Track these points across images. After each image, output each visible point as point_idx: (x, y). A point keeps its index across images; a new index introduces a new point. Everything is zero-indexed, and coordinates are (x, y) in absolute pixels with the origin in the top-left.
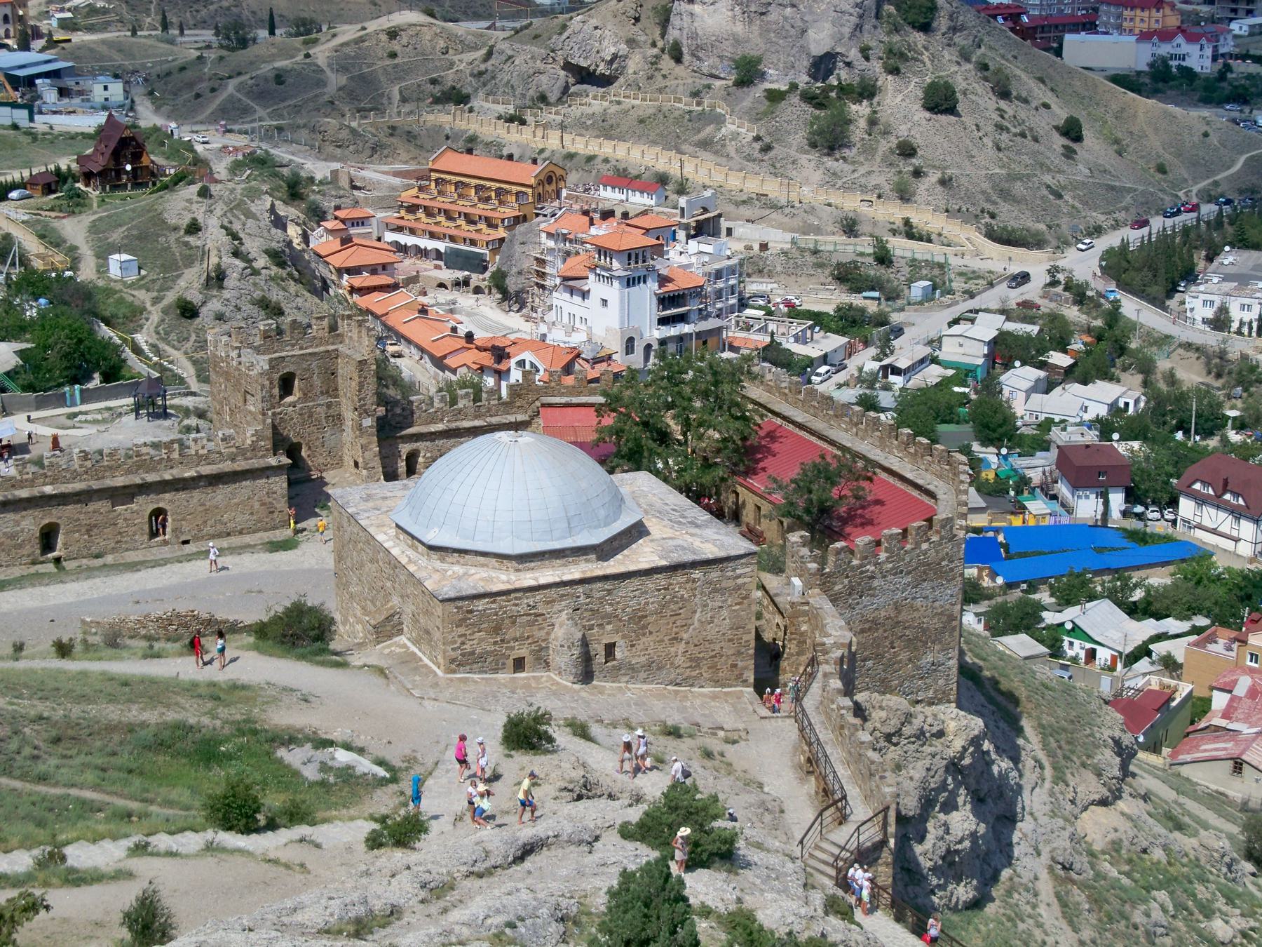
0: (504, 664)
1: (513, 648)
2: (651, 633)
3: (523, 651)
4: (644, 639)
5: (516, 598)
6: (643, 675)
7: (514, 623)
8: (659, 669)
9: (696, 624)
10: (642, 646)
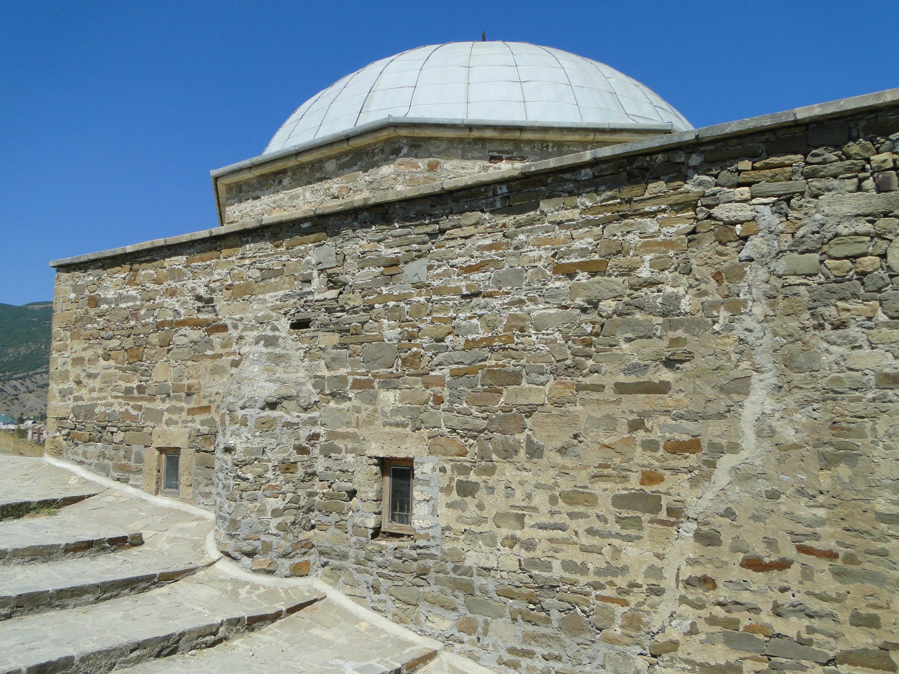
0: (140, 459)
1: (156, 416)
2: (535, 451)
3: (176, 434)
4: (507, 472)
5: (176, 275)
6: (505, 633)
7: (166, 344)
8: (573, 627)
9: (751, 448)
10: (496, 503)
